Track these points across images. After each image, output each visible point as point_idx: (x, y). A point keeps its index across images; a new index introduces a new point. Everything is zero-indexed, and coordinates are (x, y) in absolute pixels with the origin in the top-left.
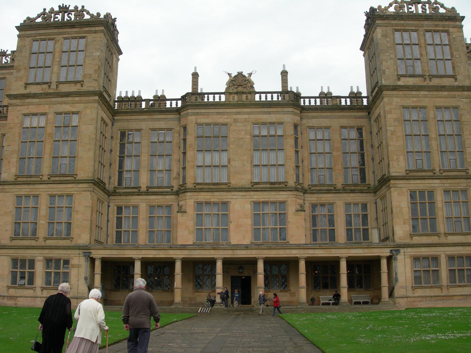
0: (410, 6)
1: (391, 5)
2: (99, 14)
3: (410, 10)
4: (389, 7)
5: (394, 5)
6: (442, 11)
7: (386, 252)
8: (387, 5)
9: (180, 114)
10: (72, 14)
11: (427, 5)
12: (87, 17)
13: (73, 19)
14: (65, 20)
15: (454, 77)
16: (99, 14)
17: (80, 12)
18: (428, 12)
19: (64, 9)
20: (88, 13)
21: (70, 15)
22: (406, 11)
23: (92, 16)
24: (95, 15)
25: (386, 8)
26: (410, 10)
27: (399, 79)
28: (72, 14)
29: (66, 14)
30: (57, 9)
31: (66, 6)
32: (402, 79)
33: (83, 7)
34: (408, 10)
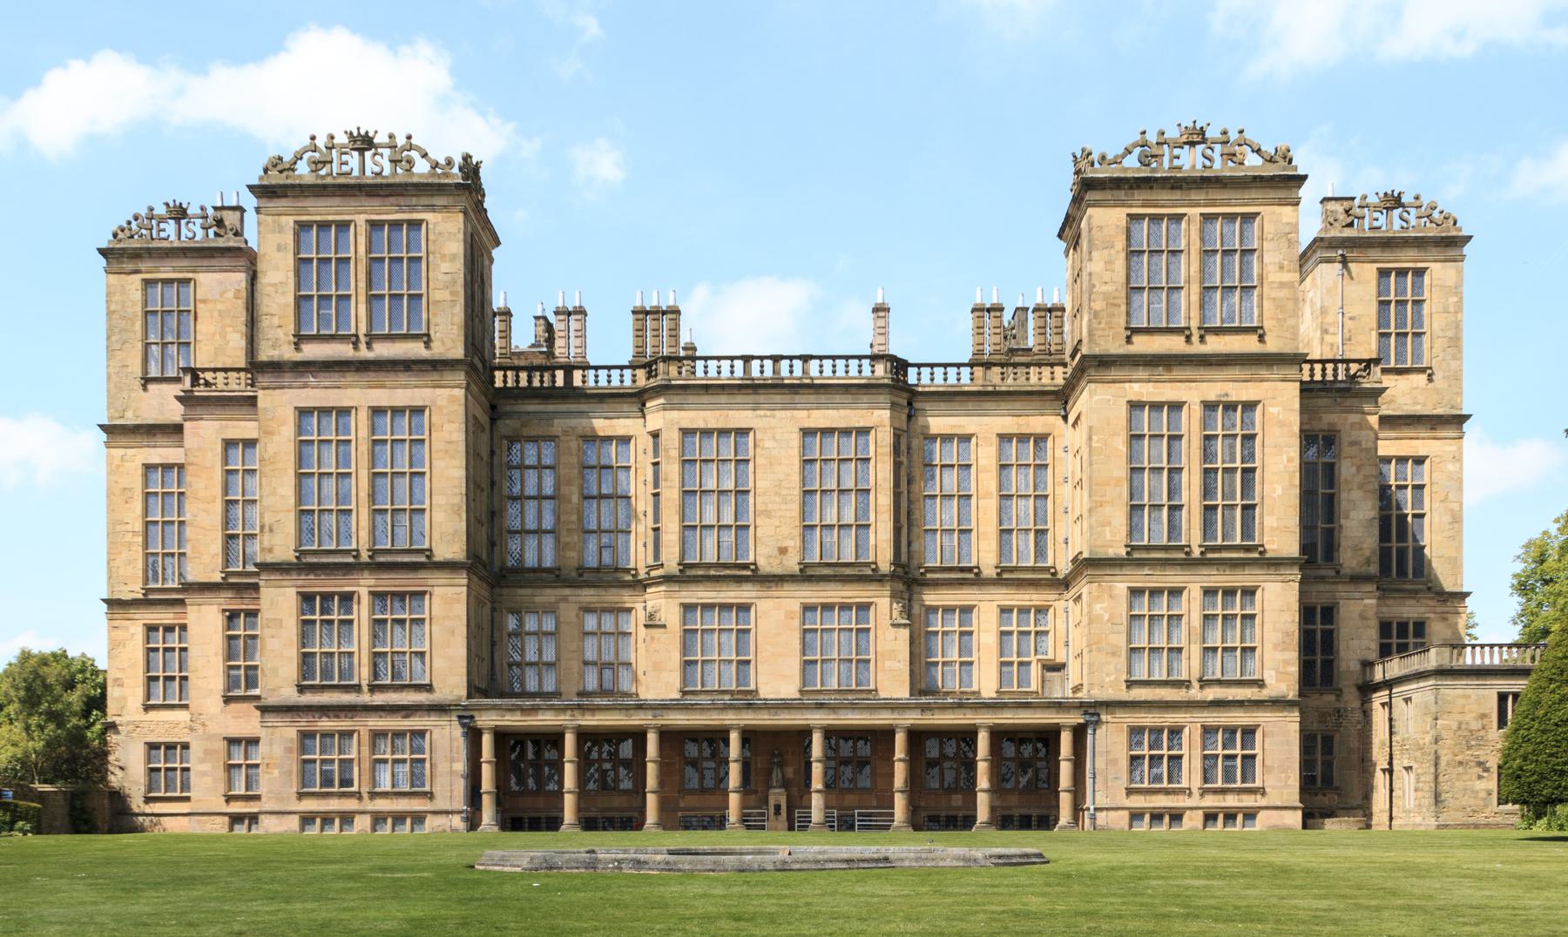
0: (1177, 152)
1: (1128, 152)
2: (449, 162)
3: (1176, 163)
4: (1124, 156)
5: (1138, 150)
6: (1252, 161)
7: (1076, 718)
8: (1121, 151)
9: (644, 405)
10: (382, 155)
11: (1218, 148)
12: (421, 167)
13: (387, 172)
14: (368, 173)
15: (1258, 332)
16: (449, 162)
17: (401, 154)
18: (1217, 165)
19: (364, 143)
20: (425, 155)
21: (378, 158)
22: (1166, 165)
23: (436, 165)
24: (442, 162)
25: (1117, 161)
26: (1175, 160)
27: (1129, 340)
28: (382, 155)
29: (368, 154)
30: (341, 139)
31: (367, 133)
32: (1135, 339)
33: (409, 137)
34: (1171, 161)
